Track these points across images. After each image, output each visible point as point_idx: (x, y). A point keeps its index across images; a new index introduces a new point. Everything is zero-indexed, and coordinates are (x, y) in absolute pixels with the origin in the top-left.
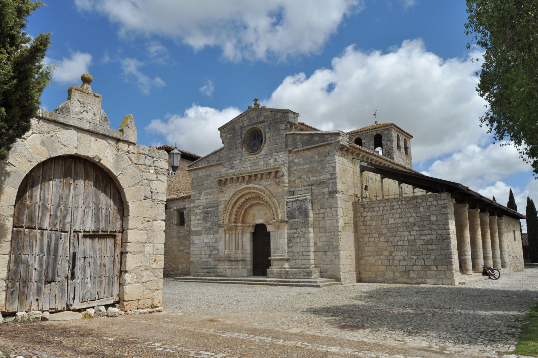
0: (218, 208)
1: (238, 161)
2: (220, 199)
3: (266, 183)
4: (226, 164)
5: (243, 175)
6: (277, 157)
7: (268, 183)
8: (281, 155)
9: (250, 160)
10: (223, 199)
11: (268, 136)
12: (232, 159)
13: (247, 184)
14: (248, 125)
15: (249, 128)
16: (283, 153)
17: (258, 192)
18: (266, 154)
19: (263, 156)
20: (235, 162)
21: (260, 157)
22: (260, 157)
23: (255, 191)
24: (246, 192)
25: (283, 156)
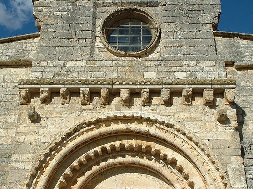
0: (9, 163)
1: (83, 63)
2: (21, 139)
3: (182, 115)
4: (43, 64)
5: (114, 87)
6: (196, 69)
7: (188, 115)
8: (208, 66)
9: (118, 65)
10: (29, 138)
11: (166, 28)
12: (66, 56)
13: (118, 109)
14: (114, 4)
15: (114, 9)
16: (210, 63)
17: (153, 130)
18: (165, 60)
19: (156, 63)
20: (69, 64)
21: (147, 63)
22: (147, 63)
23: (143, 127)
24: (114, 127)
25: (211, 68)
